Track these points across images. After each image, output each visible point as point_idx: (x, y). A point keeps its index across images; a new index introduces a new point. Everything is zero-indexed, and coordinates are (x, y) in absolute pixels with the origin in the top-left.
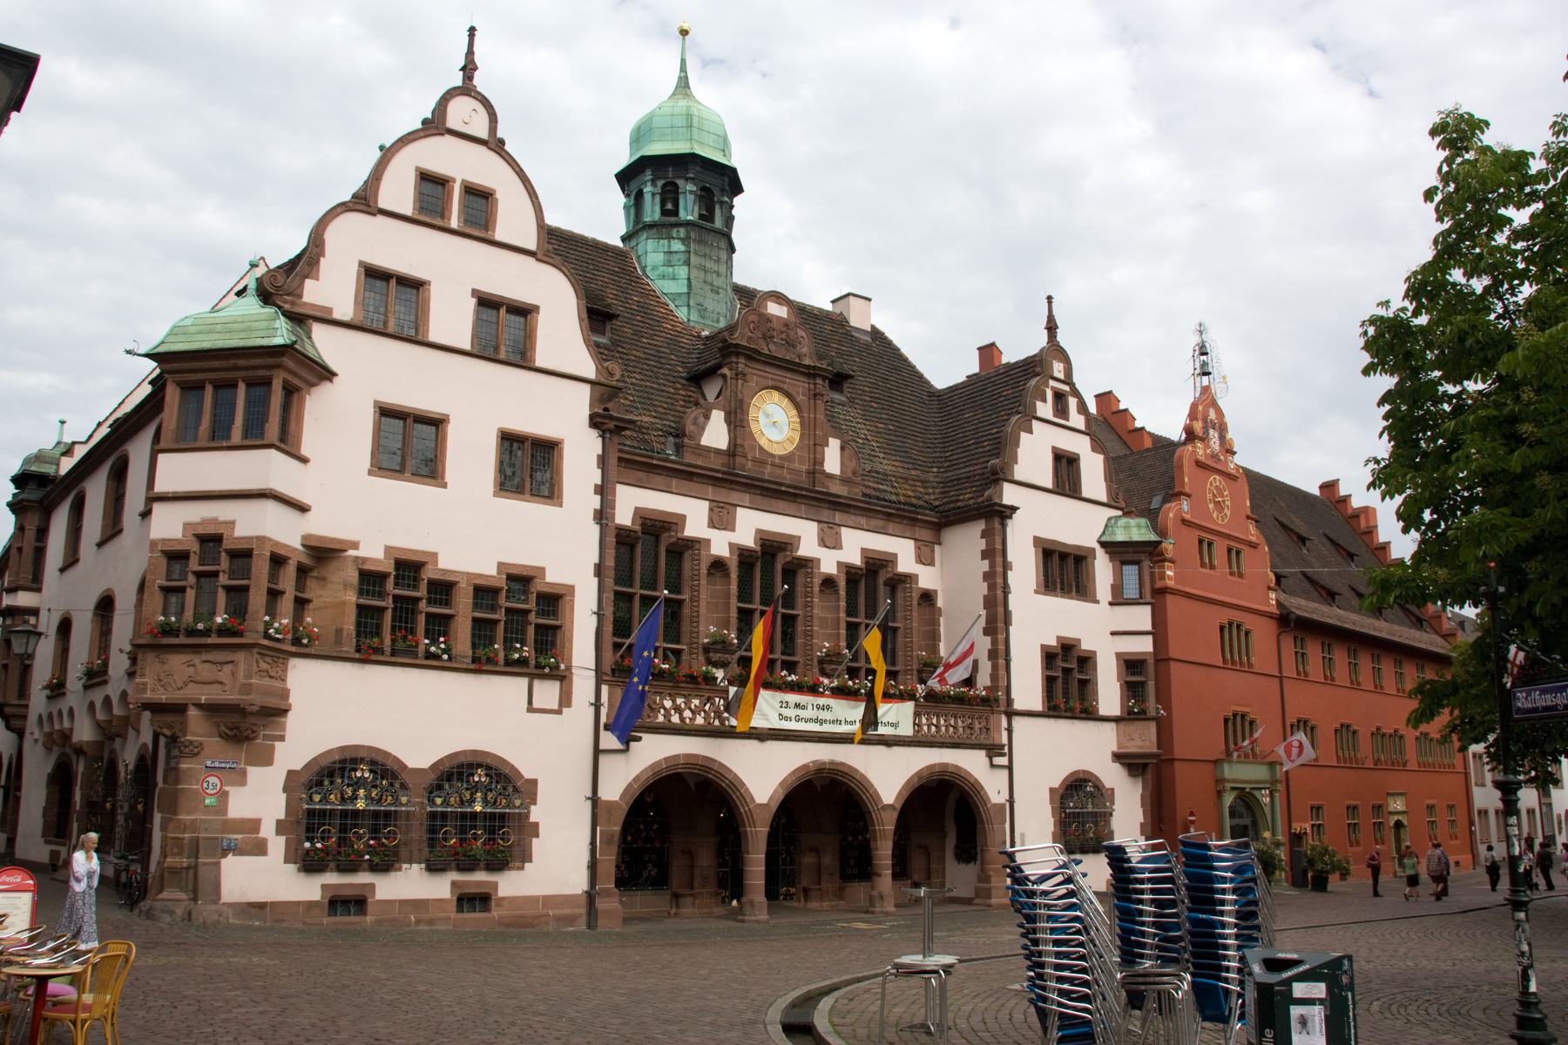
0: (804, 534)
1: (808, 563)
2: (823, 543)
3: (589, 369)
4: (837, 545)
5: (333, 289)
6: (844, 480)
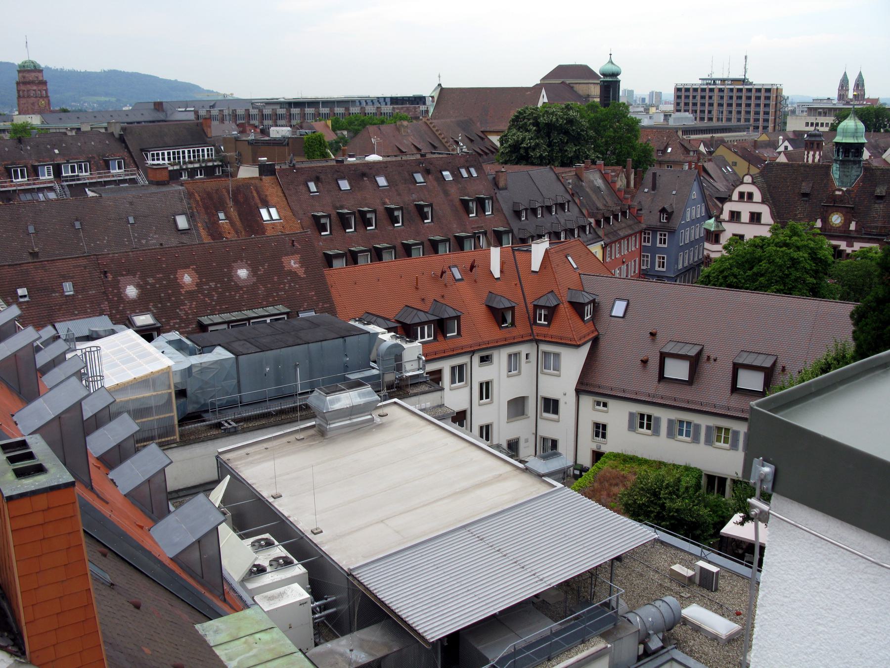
0: (843, 245)
1: (843, 251)
2: (847, 246)
3: (772, 222)
4: (852, 246)
5: (725, 216)
6: (856, 231)
